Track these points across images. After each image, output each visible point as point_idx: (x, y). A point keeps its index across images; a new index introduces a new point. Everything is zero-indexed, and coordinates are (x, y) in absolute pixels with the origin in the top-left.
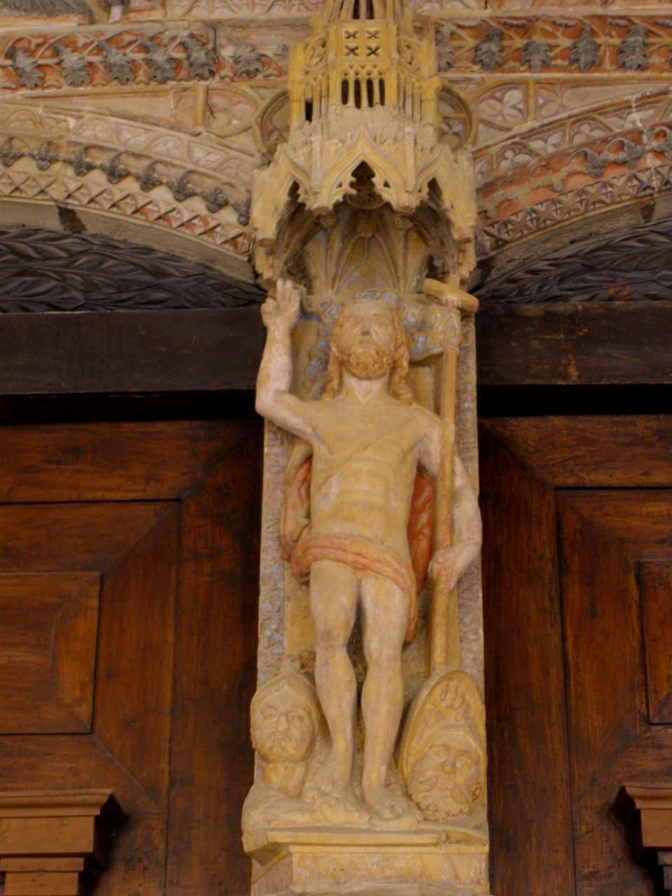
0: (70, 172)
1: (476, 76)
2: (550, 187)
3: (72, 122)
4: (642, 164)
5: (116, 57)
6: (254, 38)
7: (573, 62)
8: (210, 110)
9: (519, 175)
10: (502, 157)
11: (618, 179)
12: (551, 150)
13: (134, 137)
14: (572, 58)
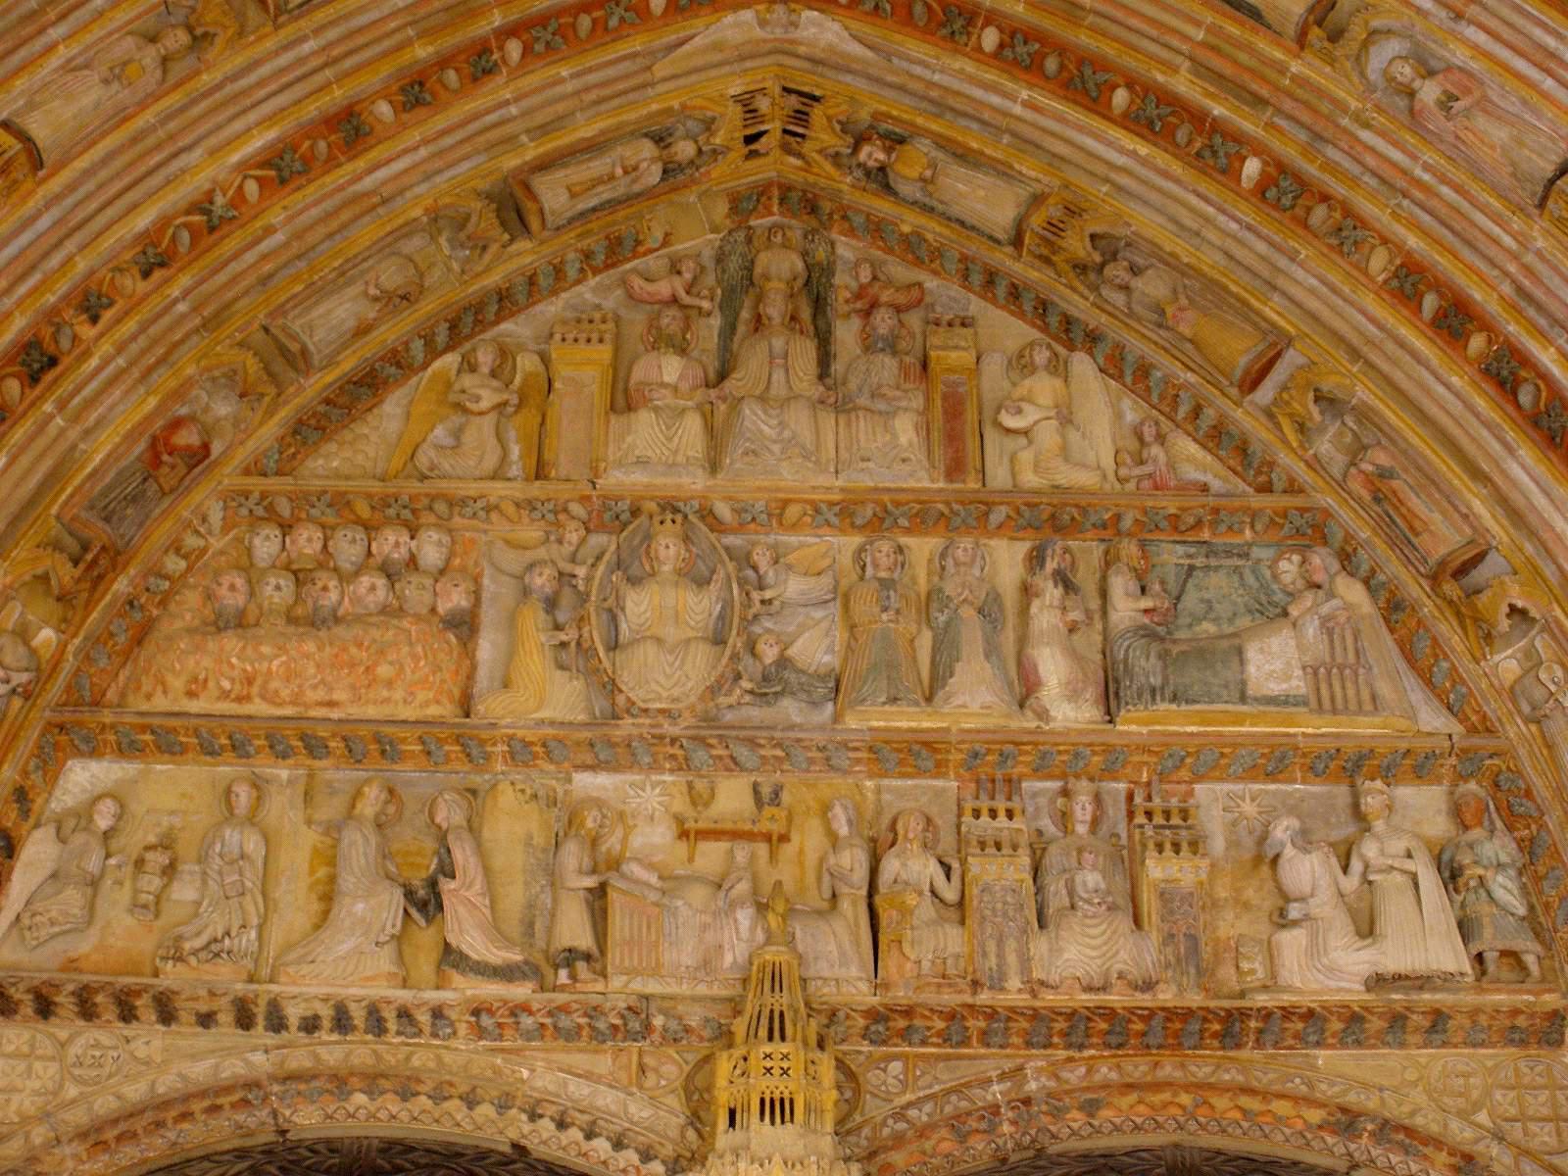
0: (524, 1117)
1: (865, 1049)
2: (924, 1153)
3: (525, 1074)
4: (999, 1130)
5: (565, 1022)
8: (642, 1069)
9: (899, 1140)
10: (884, 1123)
11: (978, 1144)
12: (925, 1118)
13: (578, 1089)
14: (946, 1039)
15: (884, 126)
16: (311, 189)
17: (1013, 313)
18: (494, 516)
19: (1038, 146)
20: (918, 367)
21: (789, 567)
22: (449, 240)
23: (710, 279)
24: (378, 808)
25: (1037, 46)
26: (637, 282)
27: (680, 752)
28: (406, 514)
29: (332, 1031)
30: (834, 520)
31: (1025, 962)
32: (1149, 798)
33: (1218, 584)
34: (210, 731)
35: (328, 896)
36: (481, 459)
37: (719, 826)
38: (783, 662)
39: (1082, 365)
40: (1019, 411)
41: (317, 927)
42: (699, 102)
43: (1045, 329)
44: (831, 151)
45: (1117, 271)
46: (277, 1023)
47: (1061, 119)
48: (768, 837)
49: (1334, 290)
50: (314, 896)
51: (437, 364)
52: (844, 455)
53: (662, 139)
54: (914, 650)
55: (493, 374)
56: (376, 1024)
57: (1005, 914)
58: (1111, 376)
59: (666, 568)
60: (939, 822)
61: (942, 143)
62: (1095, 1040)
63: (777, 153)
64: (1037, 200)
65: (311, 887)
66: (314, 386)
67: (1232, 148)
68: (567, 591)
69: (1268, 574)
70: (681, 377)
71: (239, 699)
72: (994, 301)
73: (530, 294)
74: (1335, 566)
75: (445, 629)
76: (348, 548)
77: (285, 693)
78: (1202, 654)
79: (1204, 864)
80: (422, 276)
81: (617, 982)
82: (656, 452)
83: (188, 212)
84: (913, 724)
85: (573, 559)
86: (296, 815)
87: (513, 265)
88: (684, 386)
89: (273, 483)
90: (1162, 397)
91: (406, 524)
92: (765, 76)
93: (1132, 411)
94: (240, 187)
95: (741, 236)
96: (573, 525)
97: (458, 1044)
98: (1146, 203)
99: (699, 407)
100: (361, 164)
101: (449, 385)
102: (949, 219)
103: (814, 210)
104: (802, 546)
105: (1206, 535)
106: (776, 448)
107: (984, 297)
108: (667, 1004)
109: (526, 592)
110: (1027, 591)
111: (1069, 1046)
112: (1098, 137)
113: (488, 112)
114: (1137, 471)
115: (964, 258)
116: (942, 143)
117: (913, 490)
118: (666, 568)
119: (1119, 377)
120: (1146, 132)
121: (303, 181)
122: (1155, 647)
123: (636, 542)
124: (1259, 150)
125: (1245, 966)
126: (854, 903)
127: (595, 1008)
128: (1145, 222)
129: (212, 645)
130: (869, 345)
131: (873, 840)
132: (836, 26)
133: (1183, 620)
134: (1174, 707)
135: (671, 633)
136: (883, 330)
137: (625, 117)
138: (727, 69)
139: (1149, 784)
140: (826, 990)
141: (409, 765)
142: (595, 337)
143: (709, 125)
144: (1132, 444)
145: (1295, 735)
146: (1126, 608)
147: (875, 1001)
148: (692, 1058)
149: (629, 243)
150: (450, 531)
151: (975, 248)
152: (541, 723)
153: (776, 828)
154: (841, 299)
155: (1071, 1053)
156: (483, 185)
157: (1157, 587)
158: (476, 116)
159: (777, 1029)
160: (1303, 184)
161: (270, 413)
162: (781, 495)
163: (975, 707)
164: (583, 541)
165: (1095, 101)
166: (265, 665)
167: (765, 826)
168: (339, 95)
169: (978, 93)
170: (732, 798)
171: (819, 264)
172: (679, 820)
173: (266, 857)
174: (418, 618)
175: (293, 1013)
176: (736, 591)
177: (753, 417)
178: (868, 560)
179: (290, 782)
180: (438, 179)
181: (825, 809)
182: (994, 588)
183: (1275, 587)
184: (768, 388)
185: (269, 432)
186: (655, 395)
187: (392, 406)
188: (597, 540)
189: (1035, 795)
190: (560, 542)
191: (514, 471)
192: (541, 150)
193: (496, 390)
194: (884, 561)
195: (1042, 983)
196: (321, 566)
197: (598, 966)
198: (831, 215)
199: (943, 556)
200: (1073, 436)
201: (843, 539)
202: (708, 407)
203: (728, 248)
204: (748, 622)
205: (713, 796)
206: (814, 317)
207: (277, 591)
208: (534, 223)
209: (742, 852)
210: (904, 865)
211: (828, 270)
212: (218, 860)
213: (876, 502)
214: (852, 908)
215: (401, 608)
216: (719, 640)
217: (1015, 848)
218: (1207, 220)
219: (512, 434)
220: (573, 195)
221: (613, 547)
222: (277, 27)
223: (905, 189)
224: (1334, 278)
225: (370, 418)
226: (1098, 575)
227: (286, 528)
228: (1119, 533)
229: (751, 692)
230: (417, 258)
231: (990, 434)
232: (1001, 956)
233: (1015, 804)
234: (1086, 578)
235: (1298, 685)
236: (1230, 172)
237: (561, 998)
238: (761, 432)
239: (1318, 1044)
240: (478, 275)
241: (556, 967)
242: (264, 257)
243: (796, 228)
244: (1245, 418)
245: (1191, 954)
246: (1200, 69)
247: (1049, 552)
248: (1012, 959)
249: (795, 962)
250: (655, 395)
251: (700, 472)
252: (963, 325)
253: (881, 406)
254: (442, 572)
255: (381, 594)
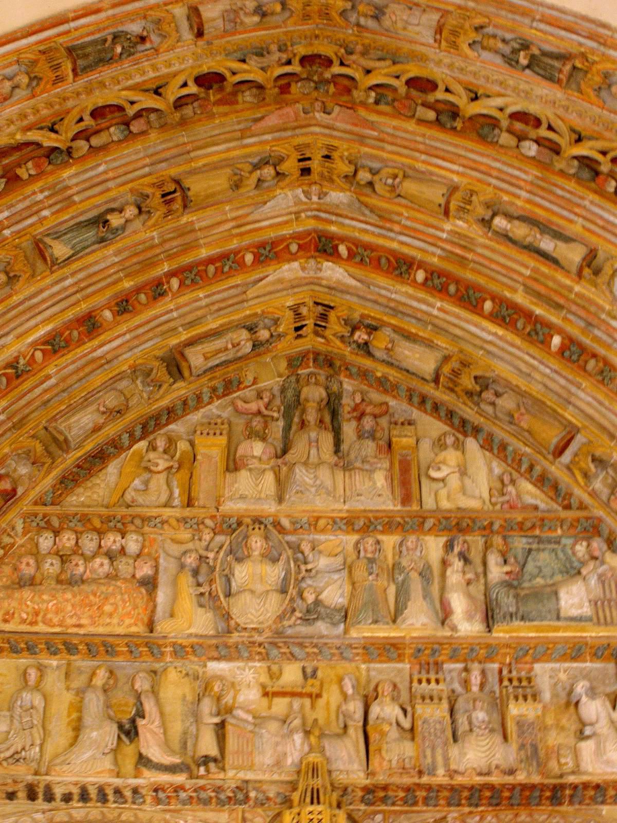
5: (203, 795)
6: (265, 787)
7: (405, 803)
14: (405, 802)
15: (369, 321)
16: (70, 356)
17: (434, 417)
18: (166, 527)
19: (446, 331)
20: (386, 447)
21: (320, 552)
22: (142, 382)
23: (278, 401)
24: (104, 681)
25: (444, 279)
26: (240, 404)
27: (263, 651)
28: (119, 525)
29: (79, 801)
30: (344, 527)
31: (446, 760)
32: (510, 672)
33: (544, 558)
34: (16, 641)
35: (77, 728)
36: (159, 495)
37: (284, 690)
38: (317, 602)
39: (471, 444)
40: (439, 469)
41: (72, 745)
42: (271, 310)
43: (452, 425)
44: (339, 334)
45: (488, 395)
46: (49, 797)
47: (458, 317)
48: (310, 695)
49: (601, 403)
50: (70, 729)
51: (136, 447)
52: (348, 493)
53: (252, 329)
54: (386, 595)
55: (165, 452)
56: (103, 797)
57: (435, 735)
58: (487, 450)
59: (256, 553)
60: (400, 686)
61: (396, 330)
62: (484, 802)
63: (311, 336)
64: (446, 359)
65: (69, 724)
66: (70, 459)
67: (546, 330)
68: (204, 566)
69: (570, 552)
70: (263, 452)
71: (31, 624)
72: (425, 412)
73: (184, 410)
74: (605, 547)
75: (140, 586)
76: (89, 543)
77: (56, 620)
78: (537, 595)
79: (540, 706)
80: (127, 400)
81: (231, 773)
82: (250, 492)
83: (5, 368)
84: (386, 635)
85: (207, 549)
86: (61, 685)
87: (174, 395)
88: (265, 458)
89: (49, 509)
90: (513, 460)
91: (119, 531)
92: (304, 295)
93: (498, 468)
94: (33, 355)
95: (293, 379)
96: (207, 531)
97: (146, 807)
98: (502, 359)
99: (272, 468)
100: (96, 342)
101: (142, 458)
102: (401, 369)
103: (331, 365)
104: (327, 541)
105: (537, 532)
106: (313, 490)
107: (419, 409)
108: (258, 785)
109: (182, 566)
110: (445, 563)
111: (470, 805)
112: (476, 325)
113: (161, 315)
114: (501, 499)
115: (409, 390)
116: (396, 330)
117: (384, 511)
118: (256, 553)
119: (491, 450)
120: (501, 322)
121: (66, 351)
122: (512, 592)
123: (240, 539)
124: (560, 331)
125: (563, 761)
126: (356, 730)
127: (219, 788)
128: (502, 369)
129: (17, 595)
130: (360, 436)
131: (366, 696)
132: (341, 270)
133: (527, 577)
134: (522, 623)
135: (259, 588)
136: (367, 427)
137: (232, 318)
138: (285, 293)
139: (510, 664)
140: (341, 777)
141: (120, 659)
142: (218, 432)
143: (276, 322)
144: (498, 485)
145: (586, 637)
146: (496, 571)
147: (368, 782)
148: (271, 814)
149: (235, 383)
150: (143, 534)
151: (415, 383)
152: (190, 635)
153: (315, 690)
154: (346, 412)
155: (472, 809)
156: (159, 353)
157: (512, 560)
158: (156, 317)
159: (315, 798)
160: (583, 349)
161: (48, 472)
162: (315, 514)
163: (418, 625)
164: (212, 539)
165: (475, 307)
166: (45, 605)
167: (308, 689)
168: (84, 307)
169: (415, 304)
170: (291, 674)
171: (334, 393)
172: (263, 686)
173: (45, 708)
174: (125, 580)
175: (58, 791)
176: (292, 565)
177: (301, 474)
178: (362, 548)
179: (57, 667)
180: (136, 350)
181: (340, 680)
182: (427, 562)
183: (574, 559)
184: (308, 457)
185: (49, 481)
186: (249, 462)
187: (112, 468)
188: (220, 539)
189: (450, 671)
190: (200, 540)
191: (176, 502)
192: (189, 335)
193: (167, 460)
194: (370, 549)
195: (456, 772)
196: (75, 553)
197: (221, 765)
198: (340, 367)
199: (401, 544)
200: (467, 481)
201: (348, 537)
202: (277, 469)
203: (287, 385)
204: (299, 581)
205: (281, 674)
206: (332, 421)
207: (51, 566)
208: (186, 373)
209: (297, 703)
210: (382, 710)
211: (339, 396)
212: (19, 709)
213: (365, 517)
214: (355, 733)
215: (116, 575)
216: (283, 591)
217: (440, 699)
218: (534, 368)
219: (175, 483)
220: (206, 359)
221: (228, 542)
222: (52, 272)
223: (379, 354)
224: (601, 397)
225: (100, 474)
226: (482, 554)
227: (56, 533)
228: (492, 532)
229: (301, 618)
230: (126, 393)
231: (424, 481)
232: (433, 757)
233: (440, 676)
234: (475, 556)
235: (587, 610)
236: (545, 343)
237: (201, 782)
238: (304, 480)
239: (603, 803)
240: (157, 400)
241: (199, 766)
242: (45, 391)
243: (322, 375)
244: (556, 470)
245: (534, 754)
246: (528, 290)
247: (456, 542)
248: (440, 759)
249: (325, 762)
250: (249, 462)
251: (273, 502)
252: (409, 424)
253: (367, 467)
254: (138, 556)
255: (106, 567)
